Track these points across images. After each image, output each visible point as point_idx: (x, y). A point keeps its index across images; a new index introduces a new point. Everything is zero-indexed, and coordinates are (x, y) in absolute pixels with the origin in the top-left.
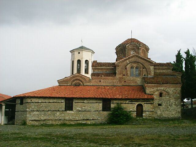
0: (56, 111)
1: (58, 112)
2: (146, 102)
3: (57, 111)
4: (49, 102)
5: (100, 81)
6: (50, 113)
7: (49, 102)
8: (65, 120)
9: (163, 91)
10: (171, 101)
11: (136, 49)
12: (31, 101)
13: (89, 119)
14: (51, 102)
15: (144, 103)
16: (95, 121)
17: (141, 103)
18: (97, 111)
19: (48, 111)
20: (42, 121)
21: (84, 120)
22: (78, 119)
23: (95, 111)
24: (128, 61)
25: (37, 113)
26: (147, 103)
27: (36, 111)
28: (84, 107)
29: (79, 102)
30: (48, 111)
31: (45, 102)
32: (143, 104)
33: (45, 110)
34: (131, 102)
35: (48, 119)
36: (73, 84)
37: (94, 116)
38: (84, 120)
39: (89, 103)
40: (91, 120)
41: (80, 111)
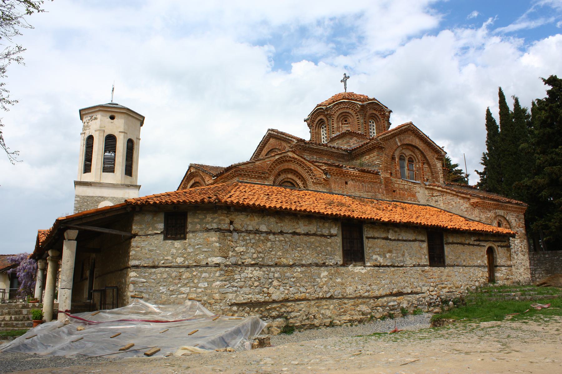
0: (317, 265)
1: (322, 269)
2: (499, 244)
3: (321, 266)
4: (294, 233)
5: (346, 183)
6: (301, 272)
7: (294, 233)
8: (344, 298)
9: (502, 220)
10: (516, 244)
11: (380, 117)
12: (231, 223)
13: (405, 291)
14: (299, 234)
15: (497, 244)
16: (418, 296)
17: (493, 246)
18: (419, 265)
19: (291, 266)
20: (274, 305)
21: (391, 295)
22: (377, 293)
23: (414, 266)
24: (397, 140)
25: (257, 273)
26: (502, 245)
27: (252, 265)
28: (390, 251)
29: (376, 235)
30: (291, 266)
31: (281, 233)
32: (495, 248)
33: (284, 261)
34: (478, 242)
35: (297, 296)
36: (277, 183)
37: (412, 280)
38: (391, 295)
39: (399, 240)
40: (408, 294)
41: (379, 266)
